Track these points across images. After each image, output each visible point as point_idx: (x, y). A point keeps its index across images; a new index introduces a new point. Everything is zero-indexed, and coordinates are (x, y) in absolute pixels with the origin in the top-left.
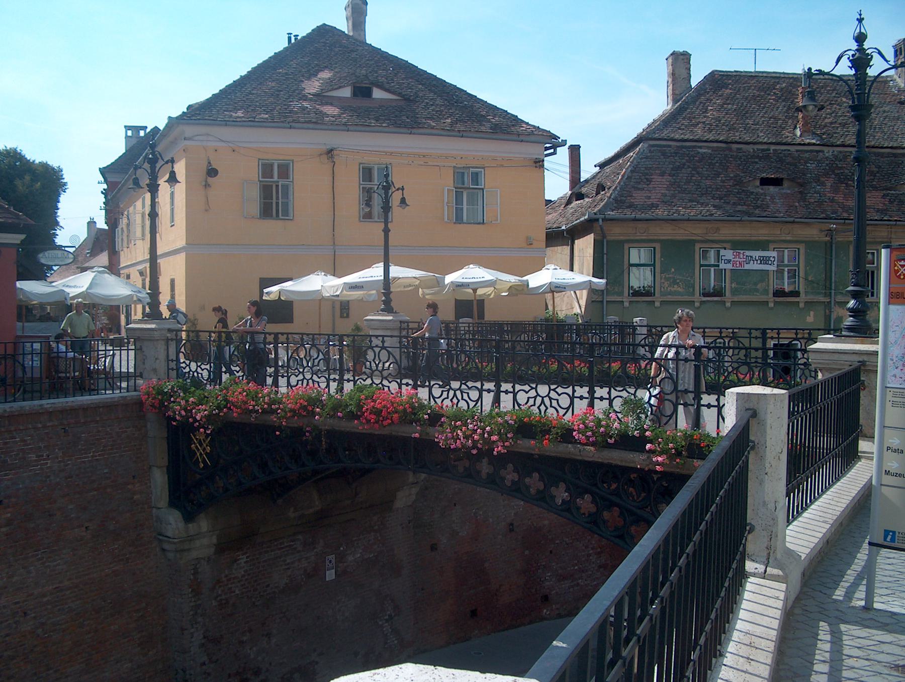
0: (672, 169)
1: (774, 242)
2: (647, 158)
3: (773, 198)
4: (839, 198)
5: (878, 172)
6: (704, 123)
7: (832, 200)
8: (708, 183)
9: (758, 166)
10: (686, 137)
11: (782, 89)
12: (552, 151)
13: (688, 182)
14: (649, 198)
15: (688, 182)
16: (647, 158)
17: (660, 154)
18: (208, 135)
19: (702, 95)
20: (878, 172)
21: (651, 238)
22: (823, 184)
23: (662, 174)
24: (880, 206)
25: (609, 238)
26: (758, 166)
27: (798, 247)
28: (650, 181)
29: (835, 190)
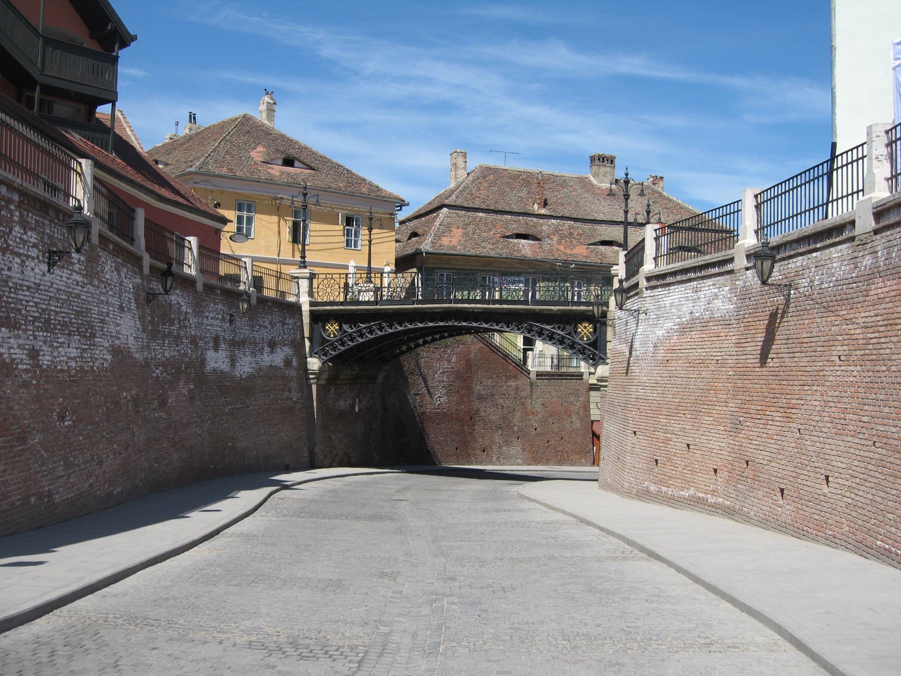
0: (464, 225)
1: (523, 273)
2: (448, 217)
3: (523, 246)
4: (562, 248)
5: (583, 234)
6: (479, 197)
7: (558, 249)
8: (485, 234)
9: (513, 226)
10: (470, 206)
11: (523, 180)
12: (399, 208)
13: (473, 234)
14: (451, 242)
15: (473, 234)
16: (448, 217)
17: (455, 215)
18: (207, 181)
19: (477, 180)
20: (583, 234)
21: (451, 266)
22: (551, 239)
23: (458, 228)
24: (585, 254)
25: (426, 266)
26: (513, 226)
27: (538, 276)
28: (451, 231)
29: (560, 243)
